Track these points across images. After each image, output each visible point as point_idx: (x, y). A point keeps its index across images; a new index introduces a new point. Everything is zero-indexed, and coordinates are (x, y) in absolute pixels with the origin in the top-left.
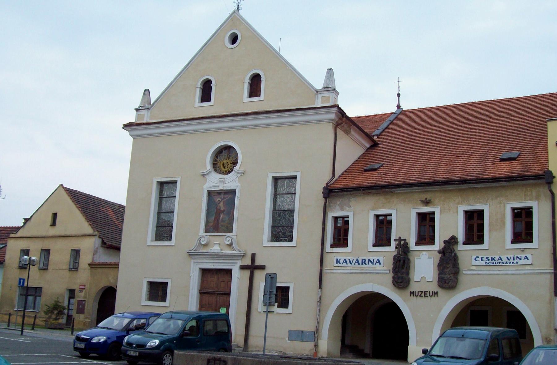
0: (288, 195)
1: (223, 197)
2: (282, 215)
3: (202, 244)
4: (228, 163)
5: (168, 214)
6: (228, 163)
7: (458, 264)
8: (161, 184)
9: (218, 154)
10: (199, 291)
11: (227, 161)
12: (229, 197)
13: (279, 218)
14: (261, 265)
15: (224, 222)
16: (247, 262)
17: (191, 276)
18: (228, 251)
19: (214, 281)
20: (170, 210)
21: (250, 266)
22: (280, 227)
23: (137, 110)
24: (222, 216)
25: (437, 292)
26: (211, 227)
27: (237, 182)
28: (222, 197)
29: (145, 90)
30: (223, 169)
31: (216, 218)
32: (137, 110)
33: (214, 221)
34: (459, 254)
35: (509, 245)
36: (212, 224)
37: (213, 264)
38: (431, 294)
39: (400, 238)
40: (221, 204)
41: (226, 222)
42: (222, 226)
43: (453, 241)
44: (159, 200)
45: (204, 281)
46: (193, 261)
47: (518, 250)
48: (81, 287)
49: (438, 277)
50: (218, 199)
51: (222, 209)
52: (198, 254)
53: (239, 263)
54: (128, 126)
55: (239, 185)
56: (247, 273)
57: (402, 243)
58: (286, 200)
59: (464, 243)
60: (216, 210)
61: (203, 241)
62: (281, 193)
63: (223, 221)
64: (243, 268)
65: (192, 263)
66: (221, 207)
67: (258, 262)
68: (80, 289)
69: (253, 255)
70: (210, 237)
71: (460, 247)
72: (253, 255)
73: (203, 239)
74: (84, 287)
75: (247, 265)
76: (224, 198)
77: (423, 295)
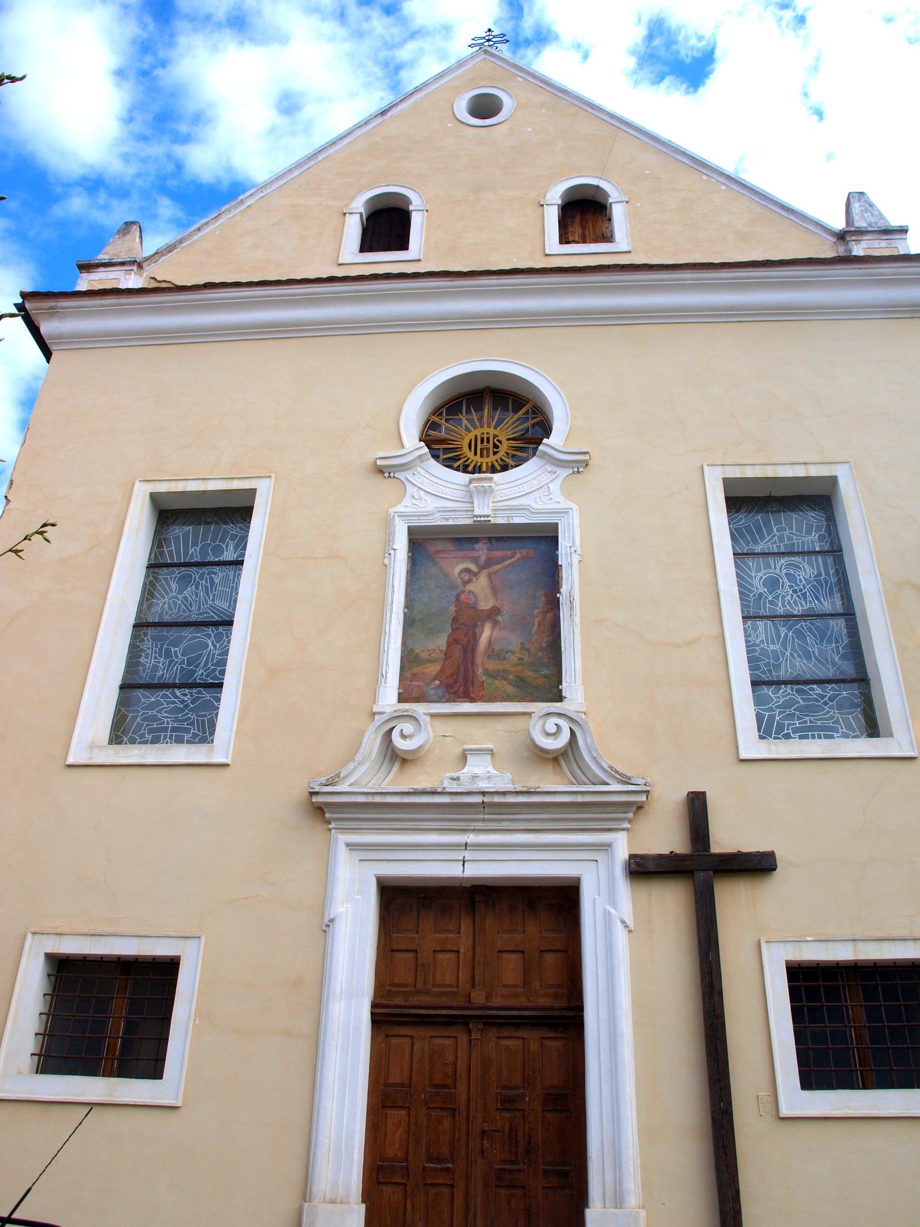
0: (796, 559)
12: (518, 555)
13: (772, 647)
15: (505, 659)
17: (332, 921)
19: (458, 952)
22: (786, 683)
24: (486, 633)
26: (434, 680)
27: (560, 498)
28: (483, 558)
31: (452, 642)
33: (448, 654)
36: (435, 669)
37: (459, 855)
40: (480, 586)
41: (513, 659)
42: (493, 675)
44: (147, 576)
45: (392, 951)
46: (343, 838)
50: (456, 566)
51: (485, 605)
52: (378, 799)
55: (574, 506)
60: (453, 609)
61: (403, 736)
62: (756, 551)
63: (493, 653)
65: (342, 850)
66: (480, 597)
70: (438, 723)
73: (408, 728)
75: (667, 852)
76: (489, 563)
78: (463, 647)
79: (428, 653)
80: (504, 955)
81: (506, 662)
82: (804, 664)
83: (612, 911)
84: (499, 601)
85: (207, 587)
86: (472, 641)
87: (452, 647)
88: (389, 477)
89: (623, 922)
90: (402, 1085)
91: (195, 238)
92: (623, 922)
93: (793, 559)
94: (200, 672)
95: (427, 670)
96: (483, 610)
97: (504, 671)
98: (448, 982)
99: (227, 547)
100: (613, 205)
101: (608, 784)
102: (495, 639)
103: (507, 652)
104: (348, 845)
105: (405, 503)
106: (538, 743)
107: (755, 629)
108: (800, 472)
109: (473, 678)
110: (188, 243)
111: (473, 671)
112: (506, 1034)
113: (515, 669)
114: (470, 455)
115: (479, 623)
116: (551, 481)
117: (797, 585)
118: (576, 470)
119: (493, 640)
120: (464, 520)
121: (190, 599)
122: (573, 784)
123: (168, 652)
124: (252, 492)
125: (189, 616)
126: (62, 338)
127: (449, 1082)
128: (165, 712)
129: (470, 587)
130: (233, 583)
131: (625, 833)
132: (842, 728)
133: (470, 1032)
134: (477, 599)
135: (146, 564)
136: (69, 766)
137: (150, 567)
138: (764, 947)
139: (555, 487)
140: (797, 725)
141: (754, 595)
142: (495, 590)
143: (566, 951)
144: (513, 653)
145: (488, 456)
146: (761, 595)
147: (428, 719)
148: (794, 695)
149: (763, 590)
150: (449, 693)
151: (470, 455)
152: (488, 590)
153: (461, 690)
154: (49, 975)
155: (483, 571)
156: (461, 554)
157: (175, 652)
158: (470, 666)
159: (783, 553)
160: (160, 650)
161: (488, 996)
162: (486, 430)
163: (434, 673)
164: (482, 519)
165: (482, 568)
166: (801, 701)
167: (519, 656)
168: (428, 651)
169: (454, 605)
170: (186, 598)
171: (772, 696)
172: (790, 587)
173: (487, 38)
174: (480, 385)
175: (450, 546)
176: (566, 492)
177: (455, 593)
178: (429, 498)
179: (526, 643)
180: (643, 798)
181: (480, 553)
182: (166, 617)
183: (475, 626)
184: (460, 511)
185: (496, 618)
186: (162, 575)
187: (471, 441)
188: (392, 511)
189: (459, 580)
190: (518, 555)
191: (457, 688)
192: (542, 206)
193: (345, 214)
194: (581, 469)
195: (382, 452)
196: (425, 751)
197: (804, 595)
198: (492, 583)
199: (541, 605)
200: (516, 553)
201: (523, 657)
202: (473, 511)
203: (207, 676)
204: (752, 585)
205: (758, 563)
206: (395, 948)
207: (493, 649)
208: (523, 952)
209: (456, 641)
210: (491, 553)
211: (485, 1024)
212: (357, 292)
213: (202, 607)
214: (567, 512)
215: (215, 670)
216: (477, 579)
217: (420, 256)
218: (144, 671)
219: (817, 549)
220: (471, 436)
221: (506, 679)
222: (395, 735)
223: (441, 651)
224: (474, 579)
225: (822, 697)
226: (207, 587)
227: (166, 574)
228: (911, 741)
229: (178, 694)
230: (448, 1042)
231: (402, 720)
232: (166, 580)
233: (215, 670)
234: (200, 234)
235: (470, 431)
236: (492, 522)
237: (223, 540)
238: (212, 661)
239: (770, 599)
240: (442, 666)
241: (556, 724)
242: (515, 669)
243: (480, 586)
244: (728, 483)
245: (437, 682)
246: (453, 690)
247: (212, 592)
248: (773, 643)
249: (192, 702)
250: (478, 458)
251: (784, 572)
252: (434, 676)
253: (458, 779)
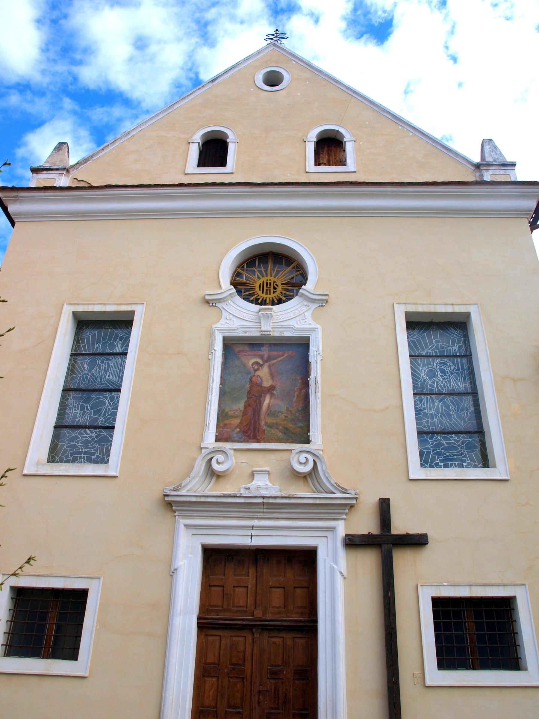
0: (446, 359)
2: (438, 405)
5: (94, 395)
12: (286, 355)
13: (430, 412)
14: (411, 532)
15: (277, 416)
17: (176, 570)
19: (247, 587)
20: (103, 384)
22: (437, 433)
24: (267, 401)
27: (311, 322)
28: (266, 356)
30: (263, 295)
31: (247, 405)
33: (244, 413)
36: (236, 421)
40: (264, 373)
41: (282, 416)
42: (270, 426)
44: (70, 360)
45: (210, 586)
46: (183, 521)
51: (267, 384)
52: (203, 500)
55: (319, 327)
60: (248, 386)
61: (218, 463)
62: (423, 355)
63: (270, 413)
66: (264, 379)
70: (239, 454)
78: (254, 409)
79: (234, 412)
80: (274, 590)
81: (278, 418)
82: (448, 422)
83: (335, 566)
84: (274, 382)
85: (105, 368)
86: (259, 405)
87: (247, 409)
88: (213, 306)
89: (341, 573)
90: (214, 663)
91: (101, 154)
92: (341, 573)
93: (444, 359)
94: (101, 419)
95: (232, 422)
96: (265, 387)
97: (277, 424)
98: (241, 604)
99: (117, 344)
100: (346, 143)
101: (335, 493)
102: (272, 405)
103: (279, 412)
104: (185, 525)
106: (295, 468)
107: (421, 401)
108: (449, 309)
109: (259, 428)
110: (97, 157)
111: (259, 424)
112: (273, 635)
113: (283, 423)
114: (260, 293)
115: (263, 395)
116: (307, 311)
117: (446, 375)
118: (321, 304)
119: (270, 405)
120: (255, 333)
121: (95, 375)
122: (315, 492)
123: (82, 406)
124: (133, 313)
125: (95, 385)
126: (20, 214)
127: (241, 662)
128: (81, 443)
129: (258, 373)
130: (121, 366)
131: (343, 521)
132: (468, 460)
133: (253, 633)
134: (262, 380)
135: (70, 353)
136: (24, 475)
137: (72, 355)
138: (420, 588)
139: (308, 314)
140: (443, 458)
141: (421, 381)
142: (272, 376)
143: (308, 588)
144: (282, 413)
145: (270, 294)
146: (425, 380)
147: (232, 452)
148: (441, 440)
149: (426, 377)
150: (245, 436)
151: (260, 293)
152: (268, 375)
153: (252, 435)
154: (12, 598)
155: (266, 363)
156: (253, 353)
157: (87, 407)
158: (257, 420)
159: (438, 356)
160: (78, 405)
161: (264, 615)
162: (269, 278)
163: (236, 424)
164: (266, 333)
165: (265, 362)
166: (445, 444)
167: (286, 415)
168: (233, 411)
169: (249, 383)
170: (93, 374)
171: (429, 440)
172: (442, 376)
173: (275, 35)
174: (267, 250)
175: (247, 348)
176: (315, 318)
177: (249, 376)
178: (235, 319)
179: (289, 407)
180: (354, 502)
181: (265, 353)
182: (82, 386)
183: (260, 396)
184: (253, 328)
185: (272, 392)
186: (79, 360)
187: (260, 284)
188: (214, 326)
189: (252, 368)
190: (286, 355)
191: (249, 433)
192: (305, 142)
193: (189, 143)
194: (324, 304)
195: (209, 291)
196: (230, 471)
198: (271, 371)
199: (299, 385)
200: (285, 353)
201: (287, 415)
202: (261, 328)
203: (105, 422)
204: (420, 375)
205: (424, 362)
206: (212, 584)
207: (271, 410)
208: (284, 588)
209: (249, 405)
210: (271, 352)
211: (262, 629)
212: (196, 193)
213: (102, 380)
214: (315, 330)
215: (109, 418)
216: (262, 369)
217: (233, 170)
218: (68, 418)
219: (458, 354)
220: (260, 281)
221: (277, 429)
222: (214, 462)
223: (241, 411)
224: (261, 368)
225: (457, 441)
226: (105, 368)
227: (82, 360)
228: (506, 470)
229: (88, 432)
230: (241, 639)
231: (218, 453)
232: (81, 363)
233: (109, 418)
234: (104, 152)
235: (260, 278)
236: (272, 335)
237: (115, 340)
238: (108, 413)
239: (430, 383)
240: (241, 420)
241: (305, 458)
242: (283, 423)
243: (264, 373)
244: (407, 314)
245: (238, 429)
246: (247, 434)
247: (108, 371)
248: (431, 409)
249: (97, 437)
250: (264, 295)
251: (438, 367)
252: (236, 425)
253: (249, 488)
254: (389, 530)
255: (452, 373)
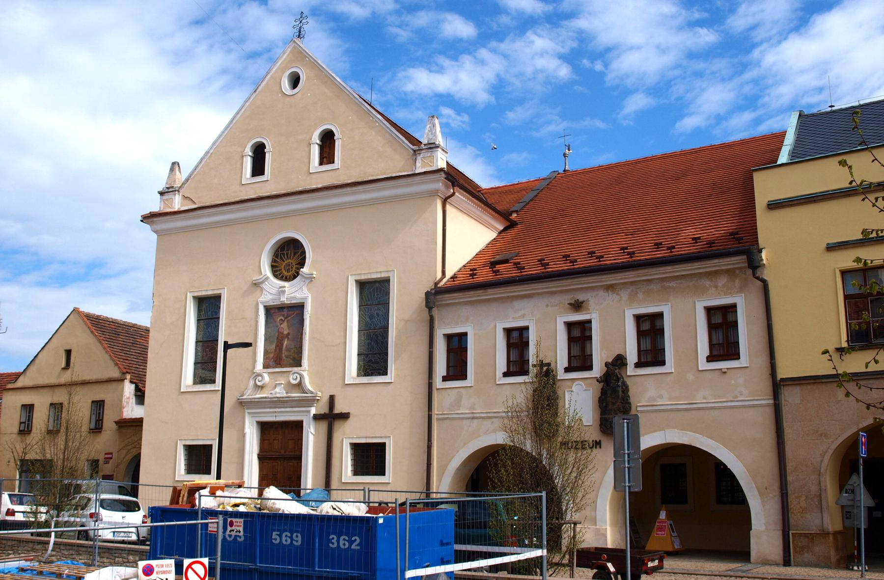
1: (287, 315)
3: (259, 386)
4: (292, 263)
6: (292, 263)
7: (629, 396)
8: (201, 301)
9: (279, 251)
10: (258, 455)
11: (291, 261)
12: (295, 313)
16: (323, 409)
18: (296, 395)
21: (328, 414)
23: (162, 193)
25: (600, 441)
28: (286, 315)
29: (174, 164)
30: (286, 273)
31: (277, 346)
32: (162, 193)
33: (275, 350)
34: (629, 382)
35: (703, 364)
38: (591, 445)
39: (541, 361)
40: (285, 325)
41: (292, 351)
43: (619, 362)
45: (264, 440)
46: (247, 411)
47: (717, 371)
48: (107, 456)
49: (600, 419)
53: (313, 411)
54: (148, 218)
56: (324, 426)
57: (545, 368)
58: (378, 314)
59: (638, 365)
60: (277, 334)
61: (259, 381)
64: (317, 418)
65: (247, 414)
67: (339, 409)
68: (105, 458)
69: (332, 398)
71: (630, 370)
72: (332, 398)
73: (260, 378)
74: (111, 456)
77: (580, 446)
89: (311, 433)
90: (266, 475)
91: (195, 173)
92: (311, 433)
101: (307, 393)
104: (248, 413)
105: (263, 297)
110: (193, 175)
114: (284, 272)
120: (277, 303)
124: (221, 294)
129: (282, 326)
136: (182, 392)
142: (289, 327)
151: (284, 272)
156: (280, 313)
161: (285, 452)
165: (285, 318)
170: (209, 331)
175: (277, 310)
183: (283, 340)
190: (295, 313)
197: (380, 321)
217: (268, 178)
221: (290, 358)
222: (257, 380)
230: (276, 464)
234: (196, 171)
253: (271, 393)
254: (332, 411)
255: (382, 315)
